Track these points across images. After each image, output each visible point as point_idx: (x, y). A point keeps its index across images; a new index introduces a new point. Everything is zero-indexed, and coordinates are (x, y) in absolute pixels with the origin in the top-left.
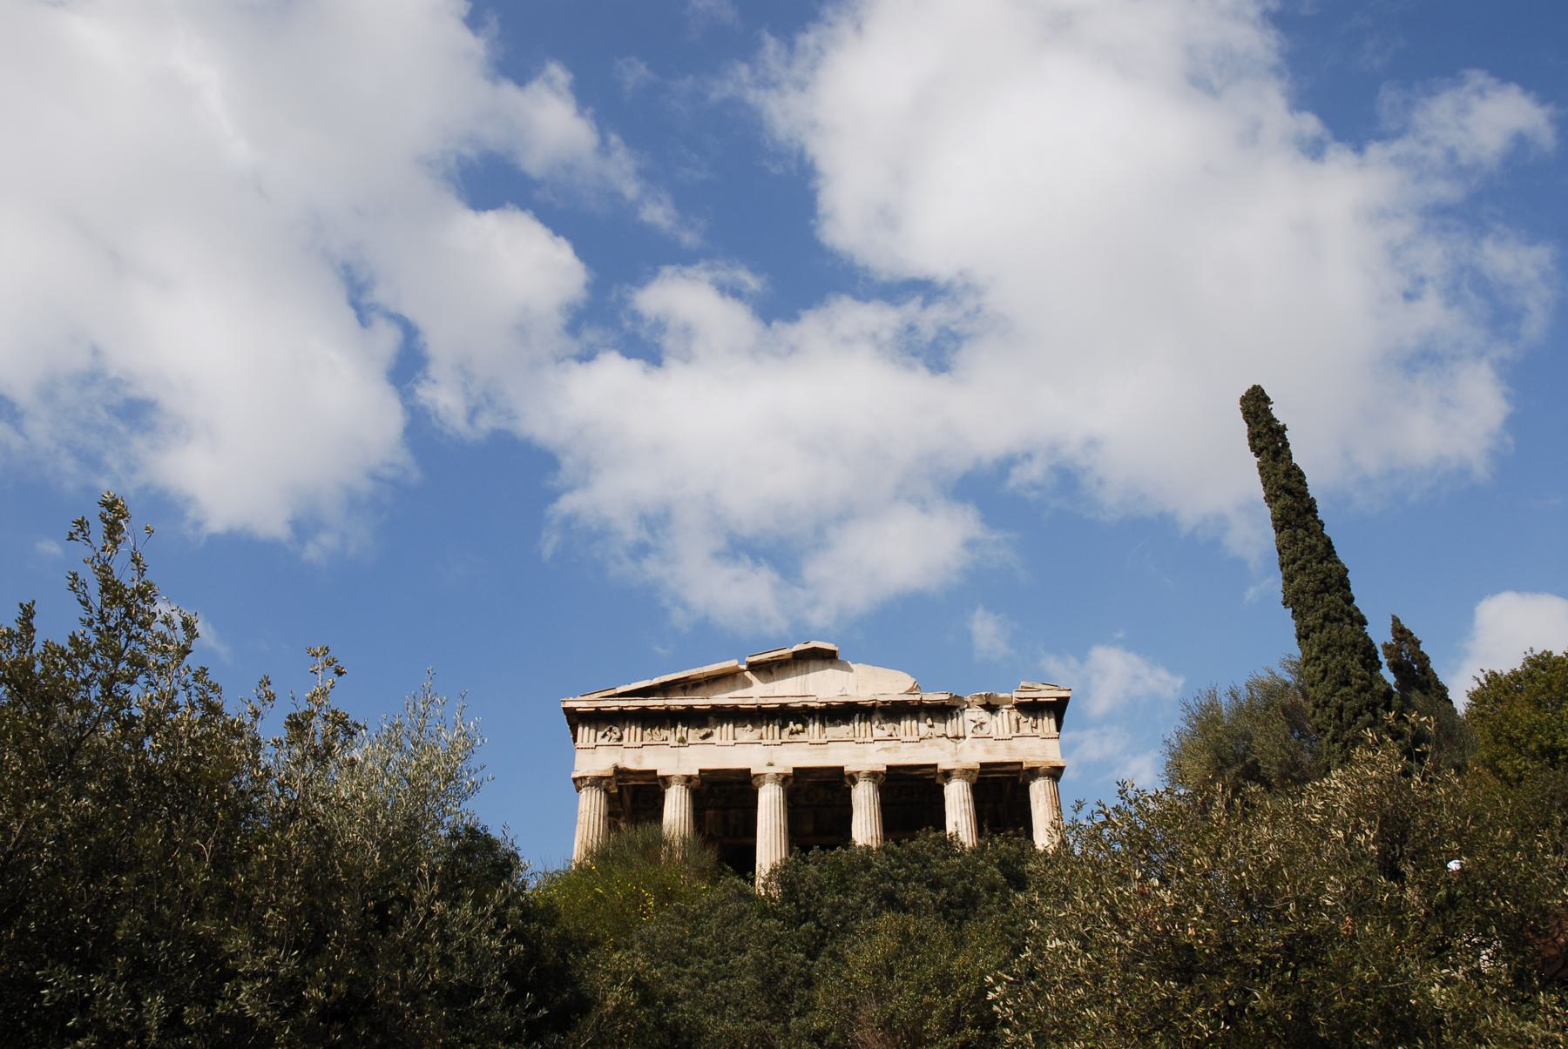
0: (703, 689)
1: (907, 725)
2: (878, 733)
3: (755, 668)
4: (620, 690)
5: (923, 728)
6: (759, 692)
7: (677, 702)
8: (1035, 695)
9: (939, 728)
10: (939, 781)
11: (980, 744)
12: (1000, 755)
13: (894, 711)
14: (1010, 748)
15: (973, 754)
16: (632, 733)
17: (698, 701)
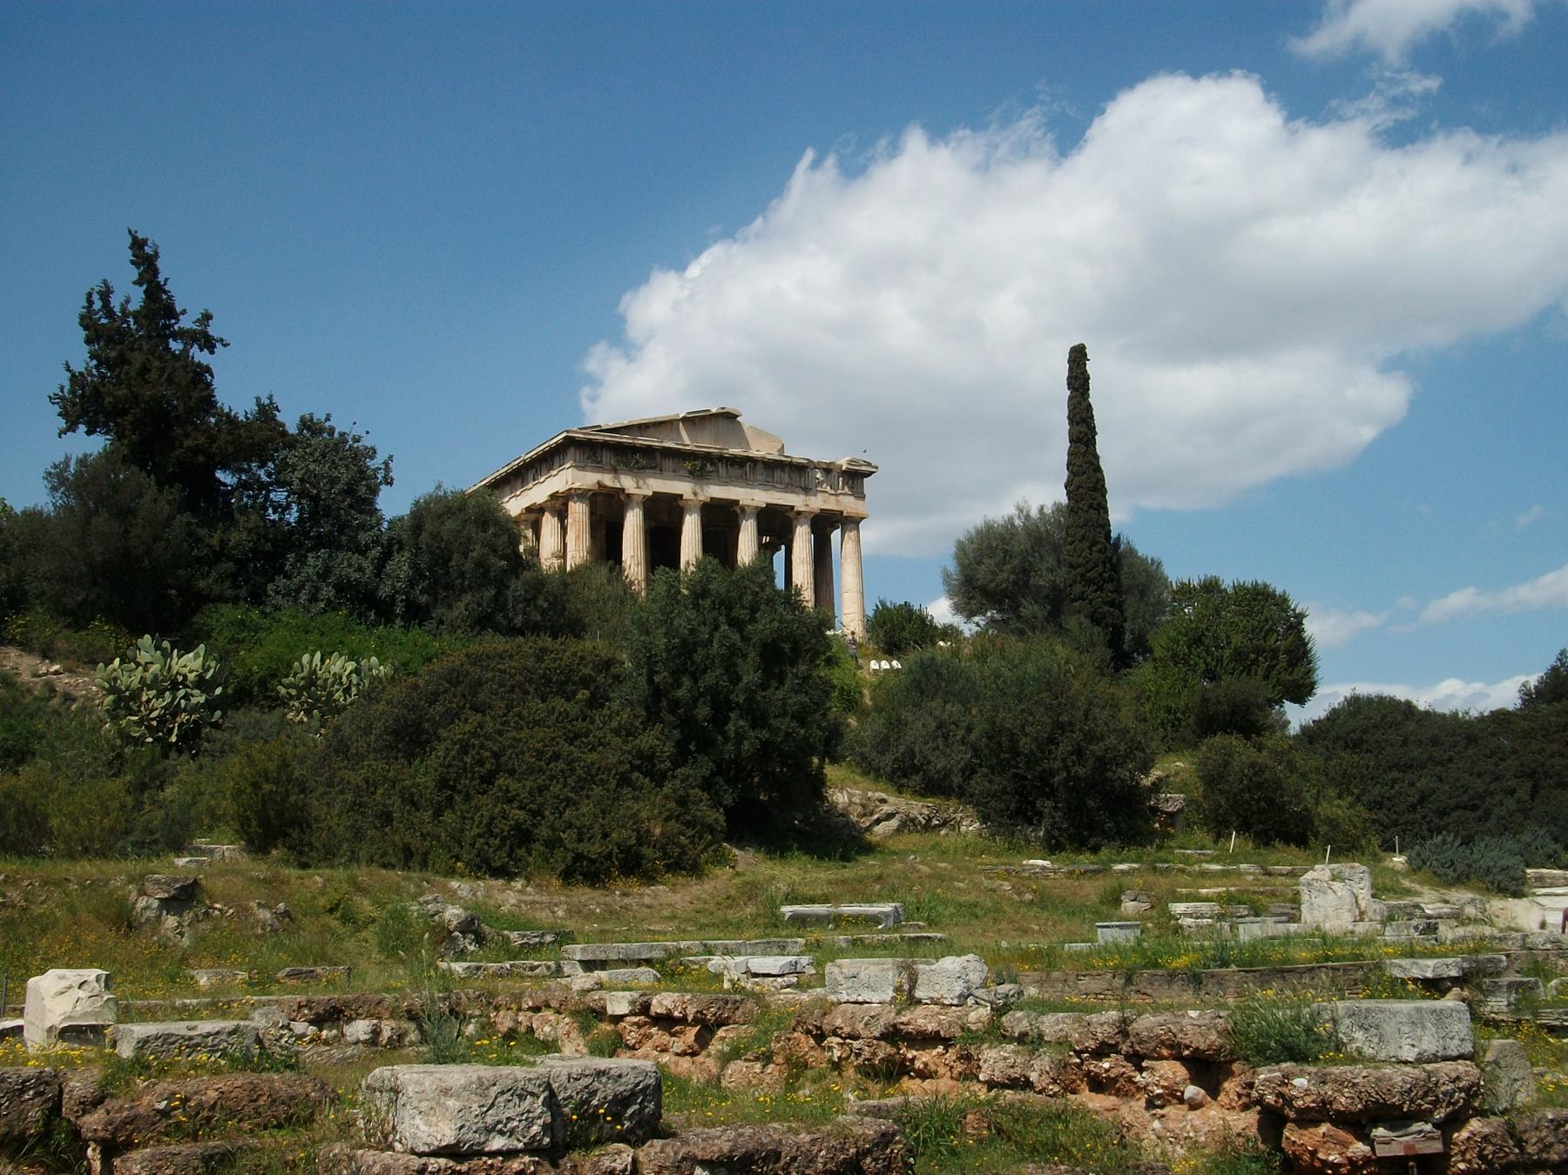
0: (651, 431)
1: (777, 473)
3: (684, 420)
6: (686, 440)
7: (642, 441)
10: (791, 515)
12: (831, 504)
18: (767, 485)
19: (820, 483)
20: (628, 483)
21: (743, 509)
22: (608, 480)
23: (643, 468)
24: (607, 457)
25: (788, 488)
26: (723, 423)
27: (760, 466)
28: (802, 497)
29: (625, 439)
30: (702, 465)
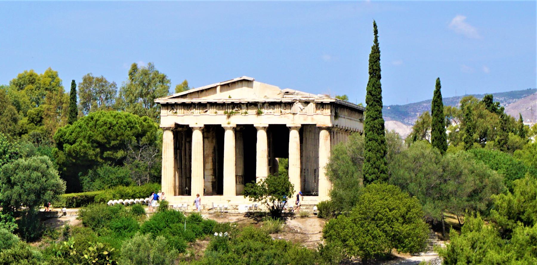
3: (222, 86)
7: (196, 100)
8: (322, 101)
9: (288, 111)
11: (302, 117)
13: (272, 104)
14: (312, 119)
16: (180, 111)
17: (204, 99)
29: (187, 100)
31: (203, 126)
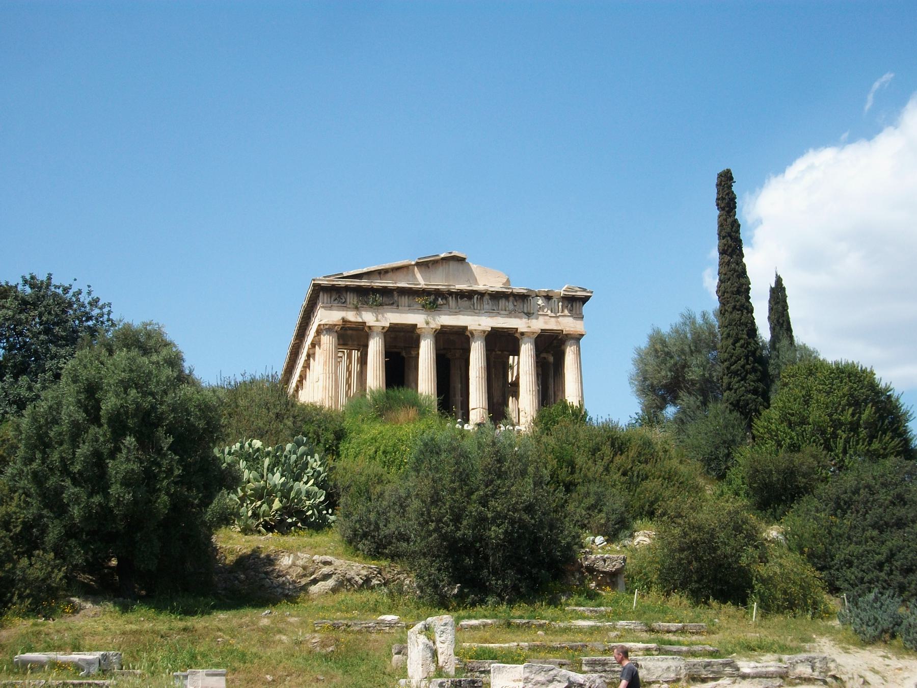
0: (390, 274)
1: (502, 303)
2: (486, 307)
3: (418, 264)
4: (345, 274)
5: (510, 306)
6: (421, 281)
7: (378, 283)
10: (517, 335)
13: (496, 296)
14: (557, 322)
15: (538, 324)
18: (492, 313)
19: (542, 308)
20: (368, 317)
21: (472, 333)
22: (351, 316)
23: (381, 305)
24: (351, 298)
25: (511, 314)
26: (453, 265)
27: (486, 297)
28: (525, 320)
29: (364, 283)
30: (434, 299)
31: (388, 325)
